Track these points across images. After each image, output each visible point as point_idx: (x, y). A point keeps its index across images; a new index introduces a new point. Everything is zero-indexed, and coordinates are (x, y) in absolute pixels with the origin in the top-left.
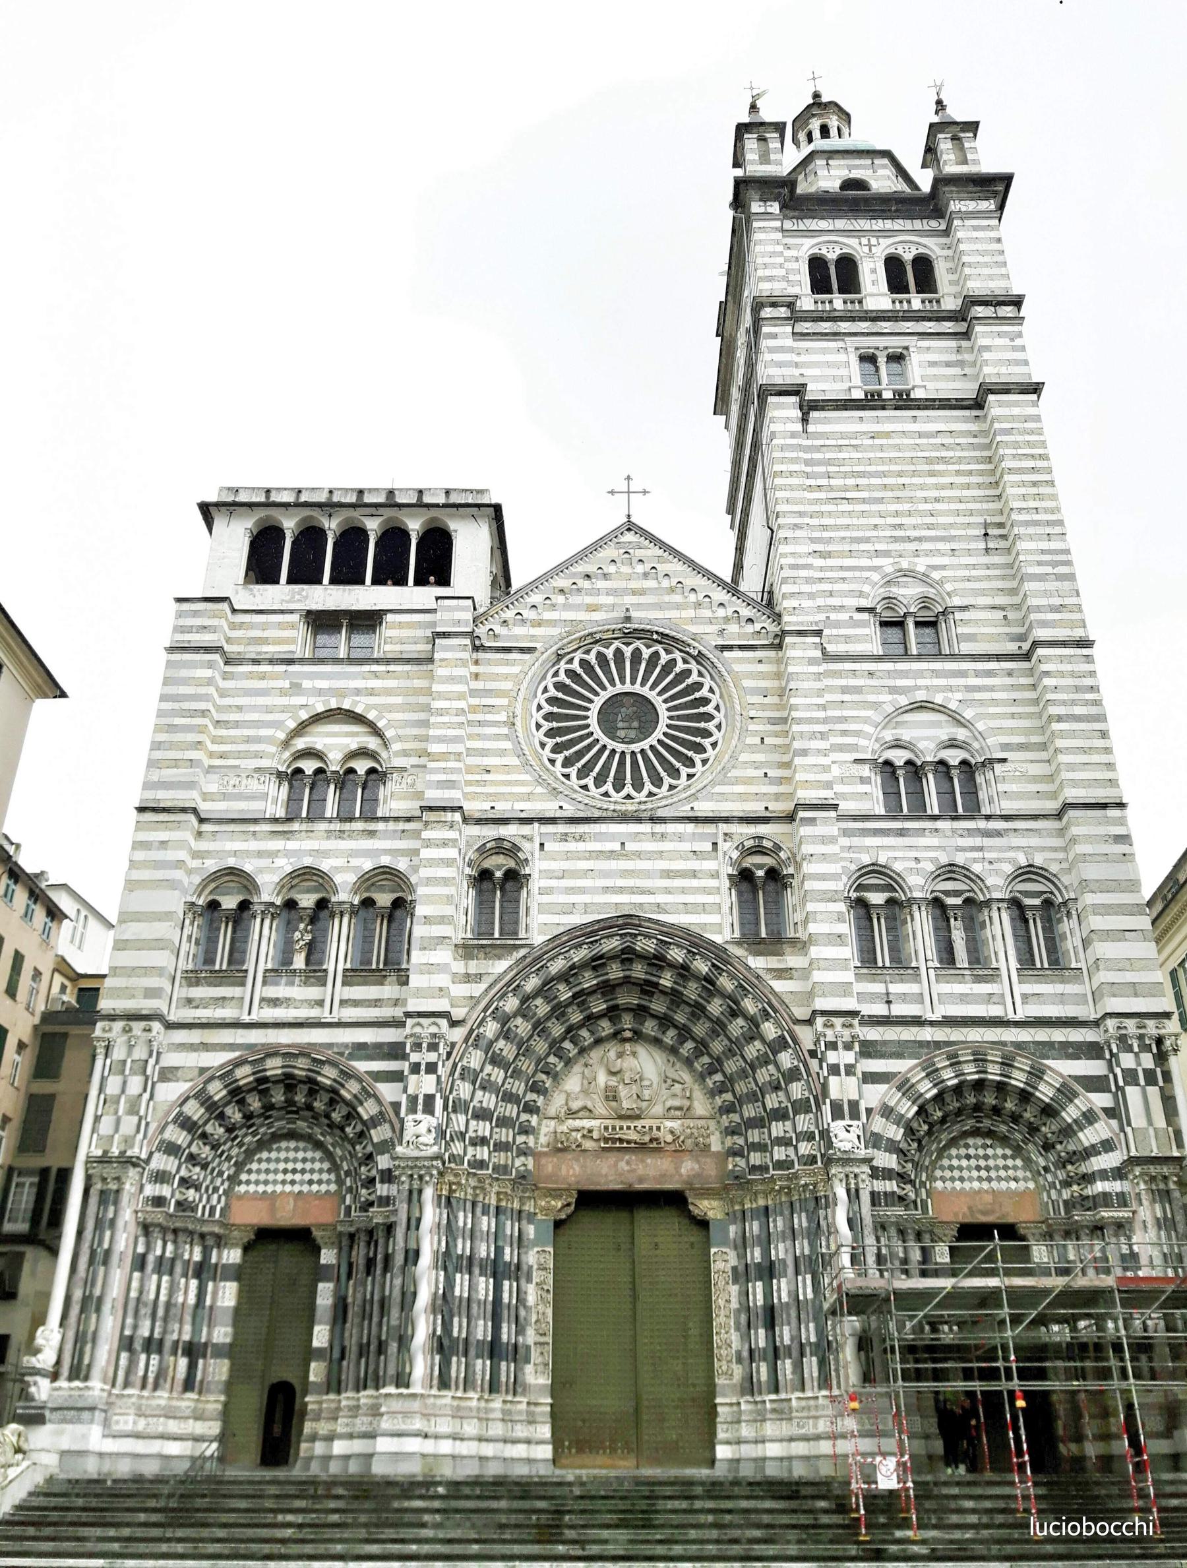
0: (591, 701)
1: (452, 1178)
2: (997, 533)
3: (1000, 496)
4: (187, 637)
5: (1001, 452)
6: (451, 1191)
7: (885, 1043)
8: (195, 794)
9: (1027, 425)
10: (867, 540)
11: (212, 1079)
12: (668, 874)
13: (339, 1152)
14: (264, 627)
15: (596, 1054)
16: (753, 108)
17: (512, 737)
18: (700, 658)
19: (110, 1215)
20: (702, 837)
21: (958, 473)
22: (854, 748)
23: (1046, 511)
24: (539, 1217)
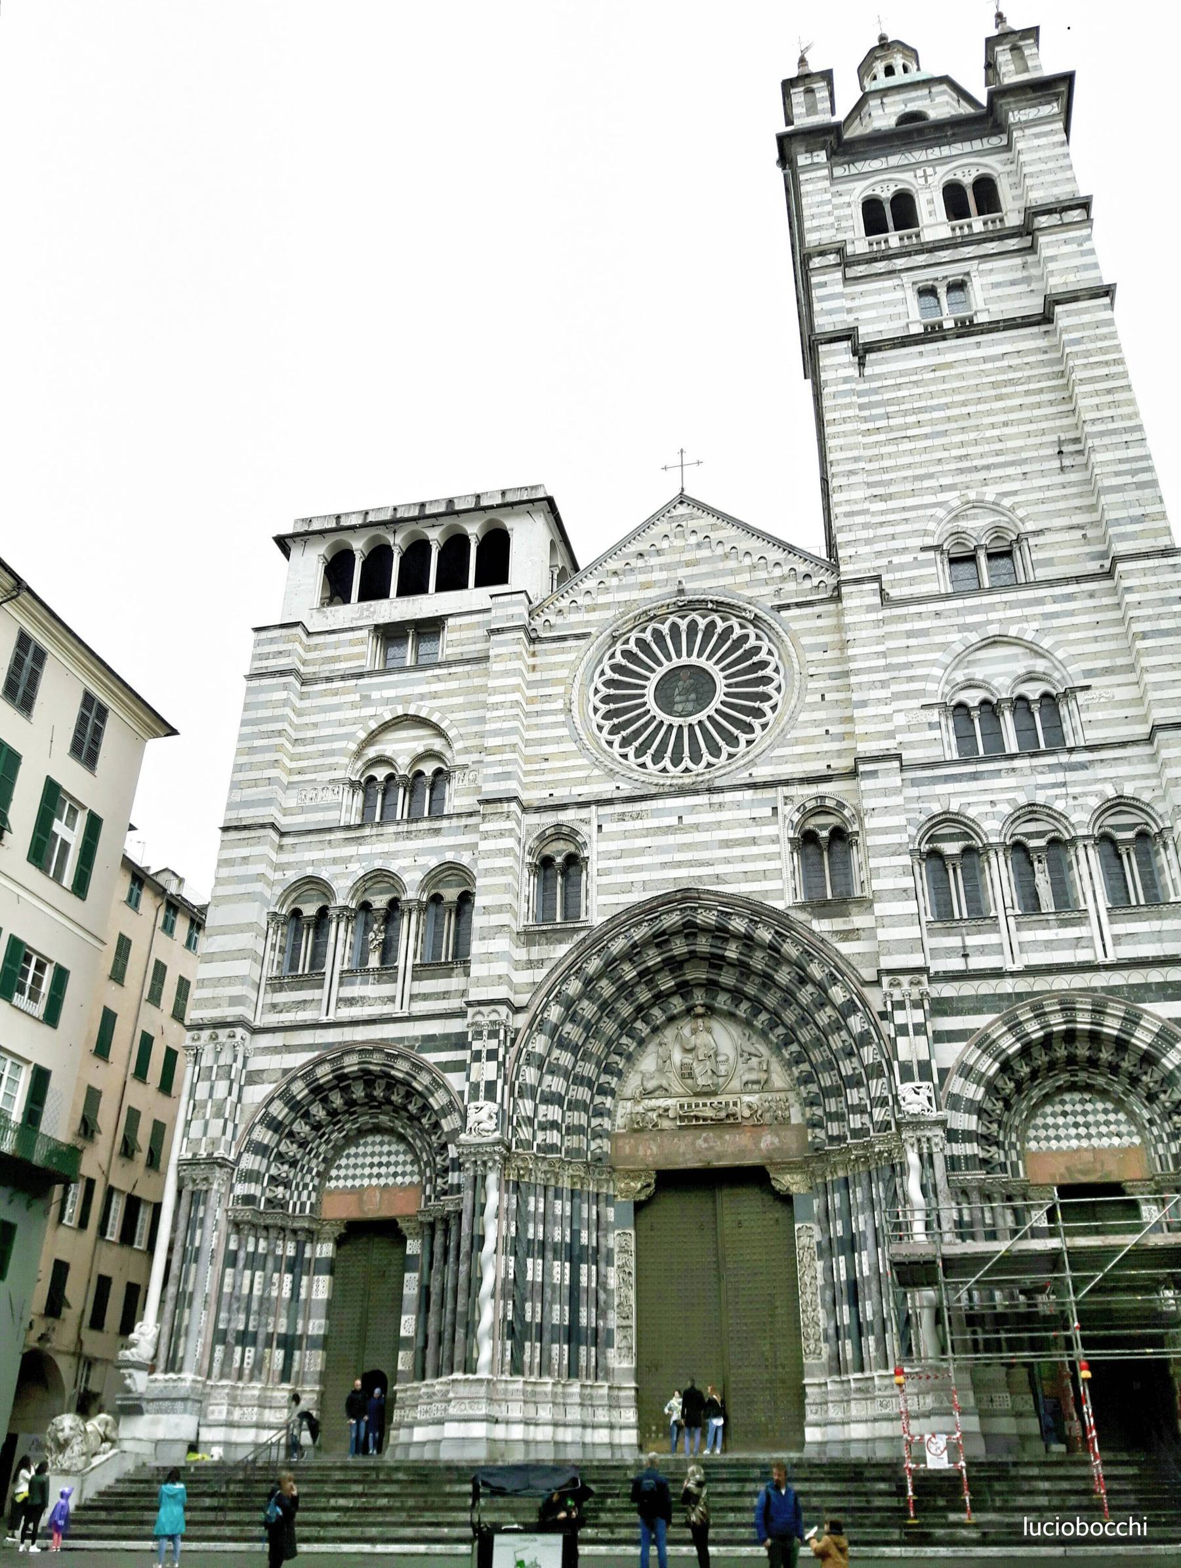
0: (647, 679)
1: (520, 1163)
2: (1071, 450)
3: (1074, 411)
4: (265, 663)
5: (1071, 363)
6: (519, 1176)
7: (961, 999)
8: (272, 810)
9: (1098, 331)
10: (930, 476)
11: (294, 1079)
12: (726, 844)
13: (418, 1143)
14: (336, 645)
15: (669, 1033)
16: (802, 61)
17: (570, 724)
18: (756, 621)
19: (201, 1215)
20: (761, 803)
21: (1027, 393)
22: (922, 693)
23: (1122, 417)
24: (619, 1199)
